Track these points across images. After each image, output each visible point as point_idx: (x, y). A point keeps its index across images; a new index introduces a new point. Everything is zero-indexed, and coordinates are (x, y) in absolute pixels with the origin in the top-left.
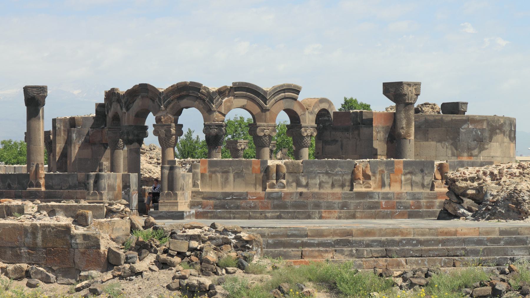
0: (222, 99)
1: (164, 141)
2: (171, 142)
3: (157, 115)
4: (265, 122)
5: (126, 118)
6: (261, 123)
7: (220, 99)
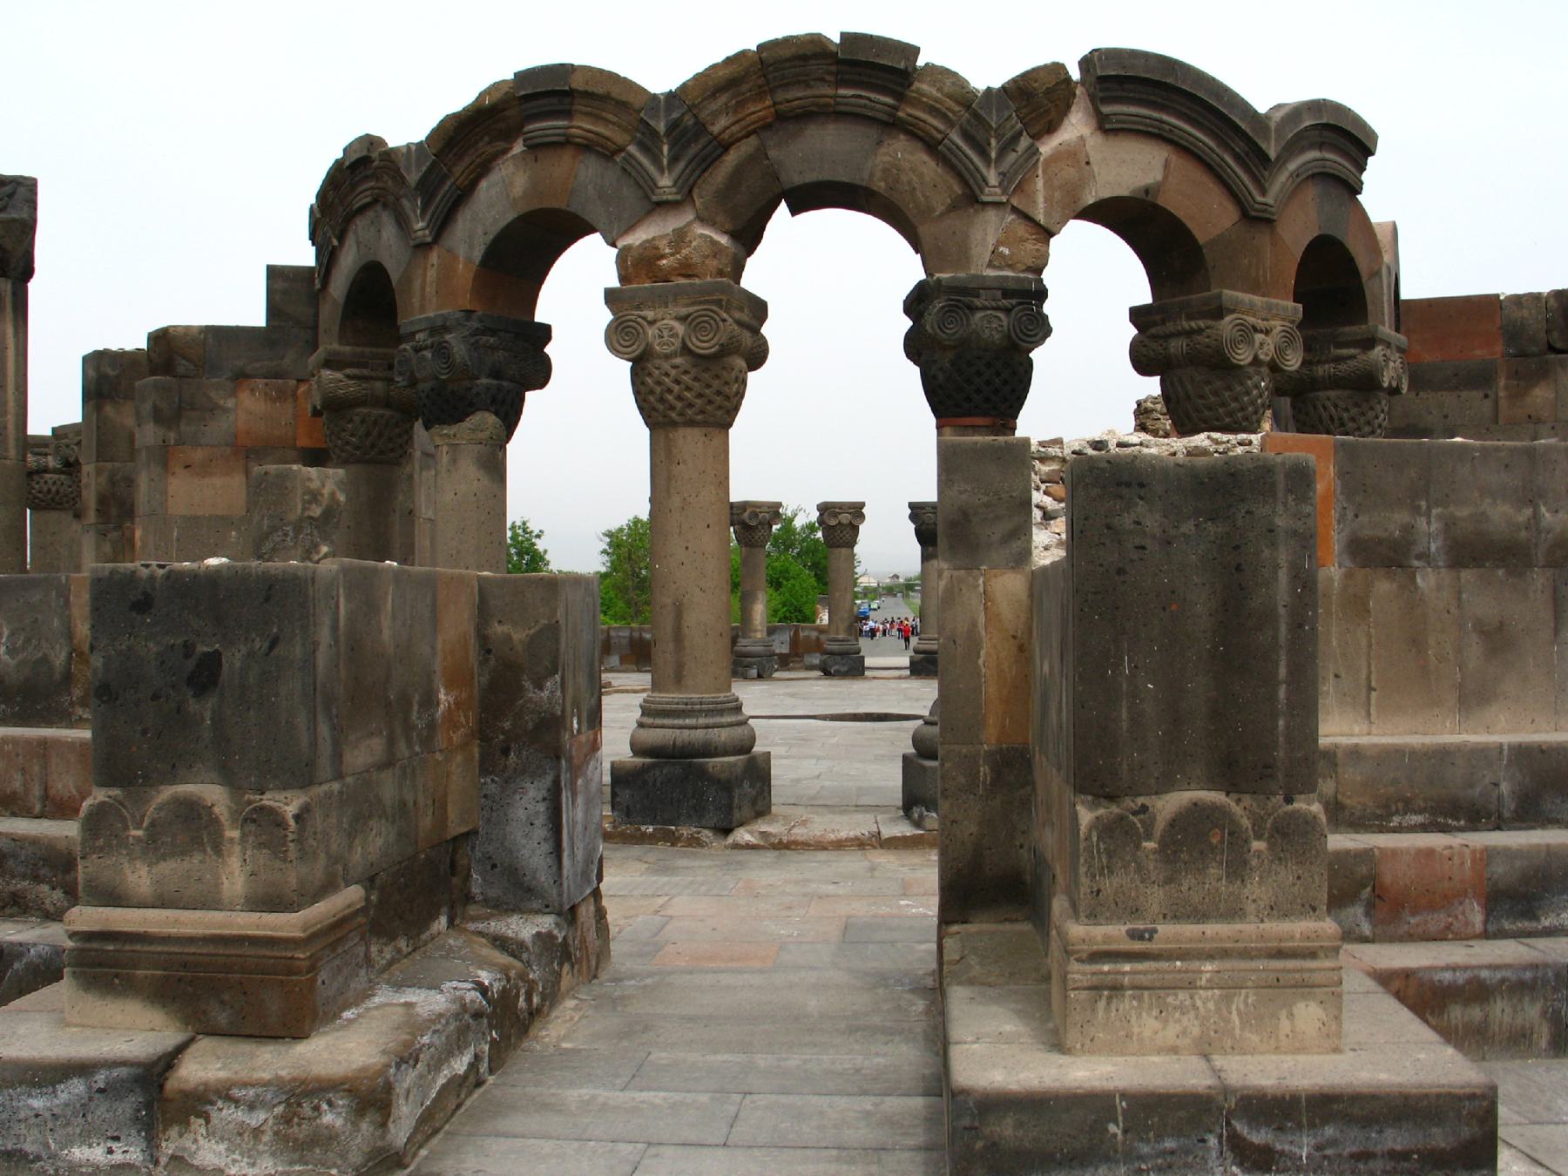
0: (1036, 137)
1: (676, 388)
2: (719, 393)
3: (620, 244)
4: (1255, 288)
5: (432, 274)
6: (1240, 295)
7: (1025, 142)
